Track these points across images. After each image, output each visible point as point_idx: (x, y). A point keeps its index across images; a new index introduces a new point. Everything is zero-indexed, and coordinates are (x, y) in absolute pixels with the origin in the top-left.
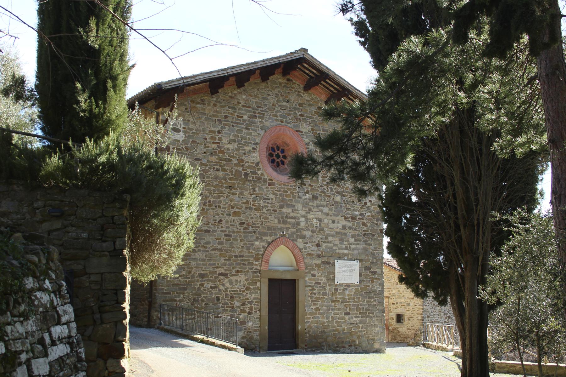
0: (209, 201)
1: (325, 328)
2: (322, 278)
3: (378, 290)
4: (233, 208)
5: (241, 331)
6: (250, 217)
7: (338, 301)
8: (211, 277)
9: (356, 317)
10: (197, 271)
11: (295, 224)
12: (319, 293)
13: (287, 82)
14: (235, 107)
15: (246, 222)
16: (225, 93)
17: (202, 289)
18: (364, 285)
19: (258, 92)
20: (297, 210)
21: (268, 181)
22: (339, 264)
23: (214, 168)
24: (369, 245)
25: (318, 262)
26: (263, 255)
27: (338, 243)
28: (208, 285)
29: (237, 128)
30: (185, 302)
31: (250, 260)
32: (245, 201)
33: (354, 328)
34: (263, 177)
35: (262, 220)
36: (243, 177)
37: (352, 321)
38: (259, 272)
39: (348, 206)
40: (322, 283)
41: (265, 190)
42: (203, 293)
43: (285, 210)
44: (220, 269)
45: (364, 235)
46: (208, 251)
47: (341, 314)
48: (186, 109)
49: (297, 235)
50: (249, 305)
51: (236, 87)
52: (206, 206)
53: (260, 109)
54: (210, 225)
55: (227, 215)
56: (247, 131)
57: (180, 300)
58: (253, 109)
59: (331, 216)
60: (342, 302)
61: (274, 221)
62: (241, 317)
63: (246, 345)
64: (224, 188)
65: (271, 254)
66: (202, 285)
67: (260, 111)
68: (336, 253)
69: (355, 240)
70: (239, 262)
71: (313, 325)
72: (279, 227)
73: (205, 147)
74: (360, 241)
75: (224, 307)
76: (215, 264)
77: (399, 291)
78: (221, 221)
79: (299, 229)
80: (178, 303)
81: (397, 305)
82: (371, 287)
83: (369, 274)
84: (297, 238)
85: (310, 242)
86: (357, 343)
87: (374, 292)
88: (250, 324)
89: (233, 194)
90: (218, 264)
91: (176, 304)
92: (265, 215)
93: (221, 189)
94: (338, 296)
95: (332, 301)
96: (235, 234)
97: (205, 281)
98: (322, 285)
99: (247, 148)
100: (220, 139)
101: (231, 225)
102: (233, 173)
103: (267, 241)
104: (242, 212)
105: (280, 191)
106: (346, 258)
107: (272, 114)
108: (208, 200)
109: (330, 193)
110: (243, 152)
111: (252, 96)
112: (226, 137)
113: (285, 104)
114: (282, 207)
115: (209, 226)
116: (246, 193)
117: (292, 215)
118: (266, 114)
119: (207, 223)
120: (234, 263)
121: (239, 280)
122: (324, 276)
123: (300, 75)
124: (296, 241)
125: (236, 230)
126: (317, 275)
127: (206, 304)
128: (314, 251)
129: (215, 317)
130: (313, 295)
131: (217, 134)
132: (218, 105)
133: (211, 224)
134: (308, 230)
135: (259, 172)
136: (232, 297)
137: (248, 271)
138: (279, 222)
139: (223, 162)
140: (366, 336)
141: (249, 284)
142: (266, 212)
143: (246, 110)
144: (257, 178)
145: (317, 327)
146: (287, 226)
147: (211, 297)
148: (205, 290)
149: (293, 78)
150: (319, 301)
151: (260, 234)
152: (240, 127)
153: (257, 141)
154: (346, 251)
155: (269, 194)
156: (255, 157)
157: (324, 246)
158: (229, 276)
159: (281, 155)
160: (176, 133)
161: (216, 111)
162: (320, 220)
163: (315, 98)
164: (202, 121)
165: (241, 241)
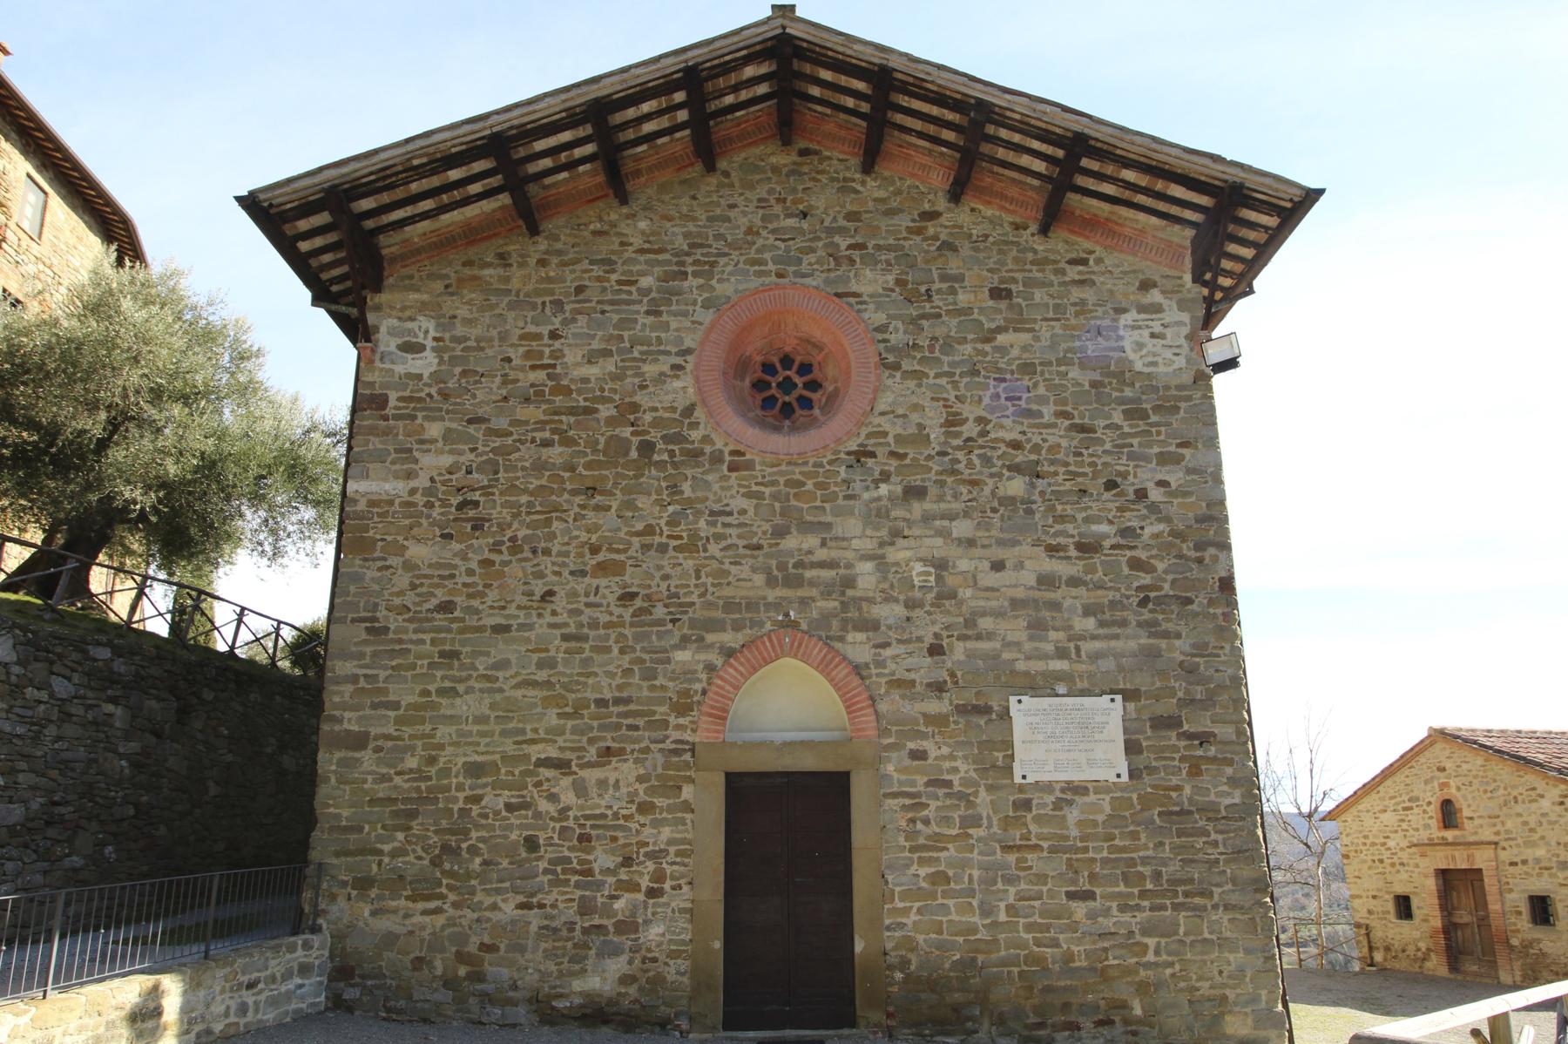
0: (513, 539)
1: (978, 951)
2: (958, 763)
3: (1228, 801)
4: (595, 550)
6: (658, 575)
7: (1037, 847)
8: (508, 773)
9: (1123, 908)
10: (457, 755)
11: (833, 585)
12: (946, 820)
13: (799, 159)
14: (613, 257)
15: (643, 592)
16: (579, 225)
17: (474, 814)
18: (1153, 787)
19: (695, 203)
20: (844, 539)
21: (727, 458)
22: (1025, 712)
23: (533, 441)
24: (1166, 635)
25: (934, 706)
26: (704, 692)
27: (1022, 636)
28: (495, 800)
29: (616, 317)
30: (411, 858)
31: (654, 713)
32: (640, 526)
33: (1118, 952)
34: (708, 449)
35: (703, 579)
36: (634, 454)
37: (1107, 923)
38: (693, 751)
39: (1059, 508)
40: (956, 783)
41: (716, 487)
42: (478, 827)
43: (791, 542)
44: (540, 747)
45: (1144, 602)
46: (501, 690)
48: (447, 287)
49: (845, 620)
51: (615, 203)
52: (500, 552)
53: (699, 251)
54: (512, 610)
55: (572, 573)
56: (652, 318)
57: (394, 849)
58: (676, 255)
59: (984, 547)
60: (1052, 850)
61: (748, 581)
62: (618, 905)
63: (637, 1006)
64: (566, 496)
65: (737, 688)
66: (477, 799)
67: (698, 257)
68: (1013, 672)
69: (1102, 624)
70: (614, 719)
71: (921, 938)
72: (770, 599)
73: (506, 381)
74: (1123, 623)
75: (554, 872)
76: (523, 732)
77: (1525, 823)
79: (854, 599)
80: (386, 860)
81: (1525, 868)
82: (1187, 791)
83: (1174, 741)
84: (844, 629)
85: (900, 641)
86: (1138, 1011)
87: (1210, 811)
88: (654, 932)
89: (598, 508)
90: (535, 731)
91: (380, 864)
92: (715, 565)
93: (554, 497)
94: (1033, 828)
95: (1007, 849)
96: (602, 632)
97: (485, 786)
99: (650, 369)
100: (557, 355)
101: (588, 605)
102: (600, 447)
103: (721, 648)
104: (630, 562)
105: (774, 483)
106: (1061, 689)
107: (742, 259)
108: (509, 534)
109: (981, 473)
110: (637, 380)
111: (670, 219)
112: (576, 345)
113: (791, 222)
114: (780, 533)
115: (507, 612)
116: (643, 502)
117: (822, 554)
118: (722, 261)
119: (502, 604)
120: (595, 723)
121: (612, 781)
122: (965, 758)
123: (840, 126)
124: (841, 639)
125: (604, 618)
126: (933, 753)
127: (485, 863)
128: (917, 670)
129: (521, 906)
130: (919, 826)
131: (546, 340)
132: (555, 260)
133: (514, 605)
134: (888, 599)
135: (695, 435)
136: (584, 838)
137: (647, 750)
138: (771, 582)
139: (564, 418)
140: (1182, 984)
141: (651, 791)
142: (718, 555)
143: (646, 262)
144: (684, 452)
145: (941, 946)
146: (800, 593)
147: (506, 837)
148: (486, 816)
149: (819, 143)
151: (693, 624)
152: (625, 311)
153: (688, 342)
155: (732, 497)
156: (682, 389)
157: (959, 651)
158: (574, 768)
159: (799, 381)
160: (409, 356)
161: (549, 280)
162: (941, 565)
163: (909, 187)
164: (497, 311)
165: (622, 651)
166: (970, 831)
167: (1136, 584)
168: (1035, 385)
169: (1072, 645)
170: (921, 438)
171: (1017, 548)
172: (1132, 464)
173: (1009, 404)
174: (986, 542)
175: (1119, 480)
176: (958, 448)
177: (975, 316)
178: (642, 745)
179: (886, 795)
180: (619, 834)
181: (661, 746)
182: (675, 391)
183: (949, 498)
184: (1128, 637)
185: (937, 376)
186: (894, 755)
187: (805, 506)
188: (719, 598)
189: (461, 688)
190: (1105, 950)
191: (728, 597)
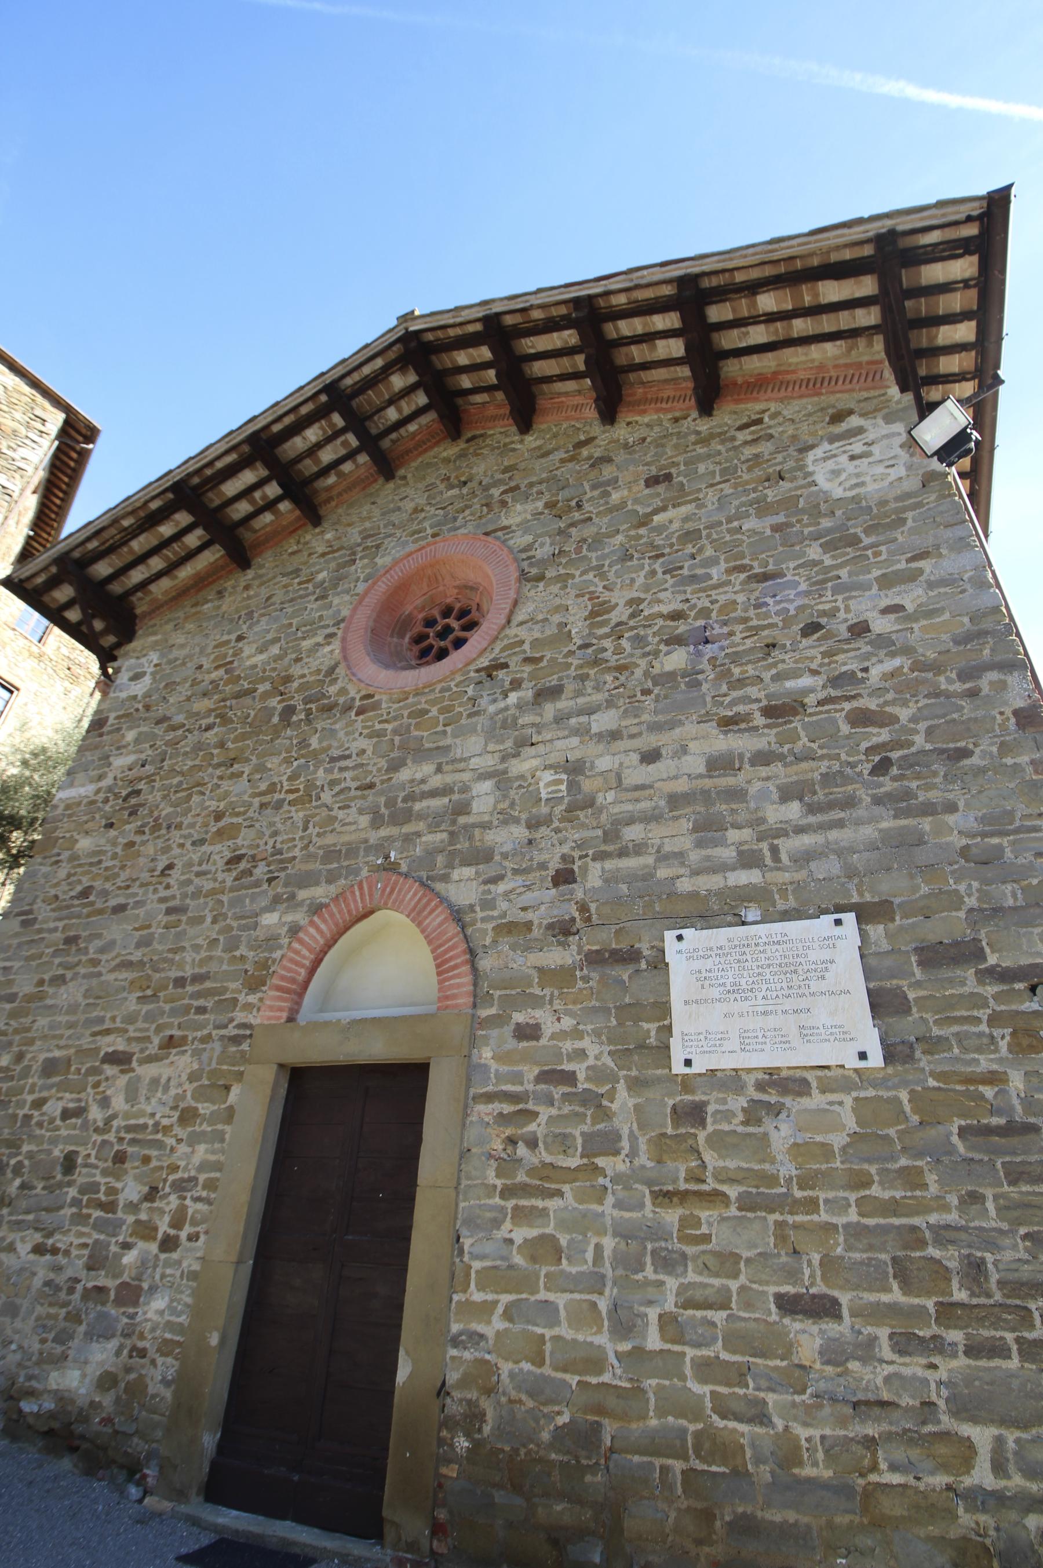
2: (585, 1043)
5: (107, 1336)
7: (716, 1197)
9: (904, 1343)
12: (563, 1142)
24: (928, 809)
25: (556, 957)
27: (686, 843)
33: (900, 1454)
40: (581, 1076)
42: (32, 1138)
45: (882, 767)
46: (100, 974)
47: (748, 1306)
49: (452, 854)
50: (174, 1201)
59: (632, 736)
60: (747, 1204)
62: (129, 1258)
68: (672, 895)
74: (850, 803)
76: (101, 1020)
78: (170, 867)
79: (465, 827)
82: (1017, 1082)
83: (971, 985)
85: (516, 872)
94: (710, 1157)
97: (52, 1086)
98: (581, 1086)
99: (306, 644)
106: (752, 914)
109: (632, 655)
113: (455, 492)
117: (436, 781)
121: (163, 1081)
122: (597, 1033)
124: (445, 878)
126: (549, 1027)
127: (23, 1186)
128: (535, 908)
130: (522, 1150)
133: (138, 883)
134: (508, 820)
138: (377, 821)
141: (198, 1095)
145: (537, 1389)
146: (407, 829)
149: (483, 428)
150: (560, 1193)
154: (749, 877)
157: (594, 875)
162: (575, 769)
166: (601, 1162)
167: (864, 745)
168: (701, 550)
169: (765, 846)
170: (563, 634)
171: (677, 731)
172: (840, 598)
173: (668, 577)
174: (634, 730)
175: (823, 621)
176: (607, 636)
177: (630, 507)
178: (205, 1032)
179: (477, 1098)
180: (154, 1153)
181: (223, 1032)
182: (324, 656)
183: (589, 691)
184: (859, 823)
185: (582, 574)
186: (494, 1033)
187: (425, 734)
188: (319, 848)
189: (69, 975)
190: (870, 1443)
191: (329, 846)
